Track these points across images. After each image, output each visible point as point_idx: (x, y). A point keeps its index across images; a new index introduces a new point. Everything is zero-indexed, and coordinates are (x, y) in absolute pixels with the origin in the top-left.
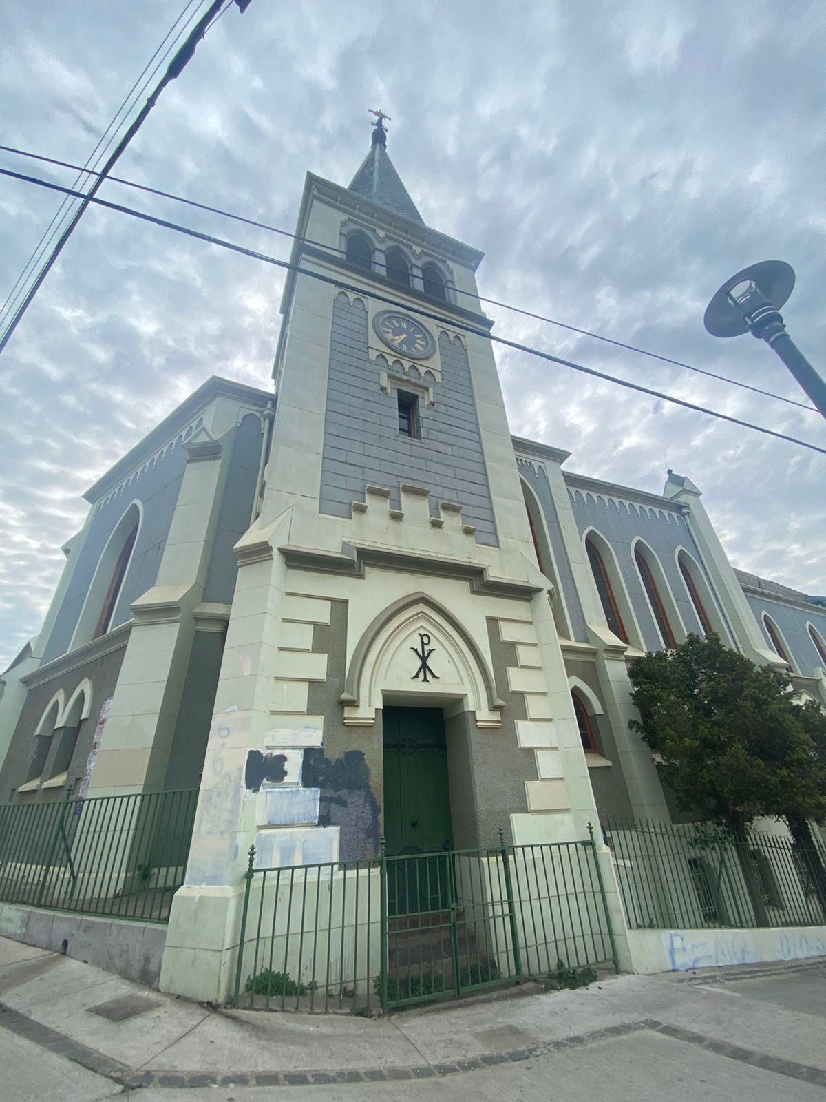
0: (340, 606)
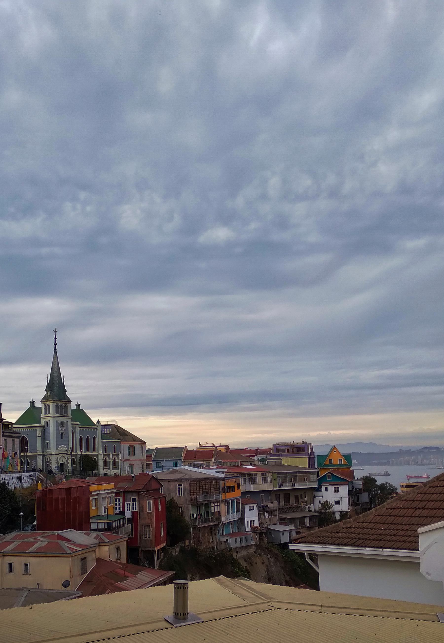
0: (58, 457)
